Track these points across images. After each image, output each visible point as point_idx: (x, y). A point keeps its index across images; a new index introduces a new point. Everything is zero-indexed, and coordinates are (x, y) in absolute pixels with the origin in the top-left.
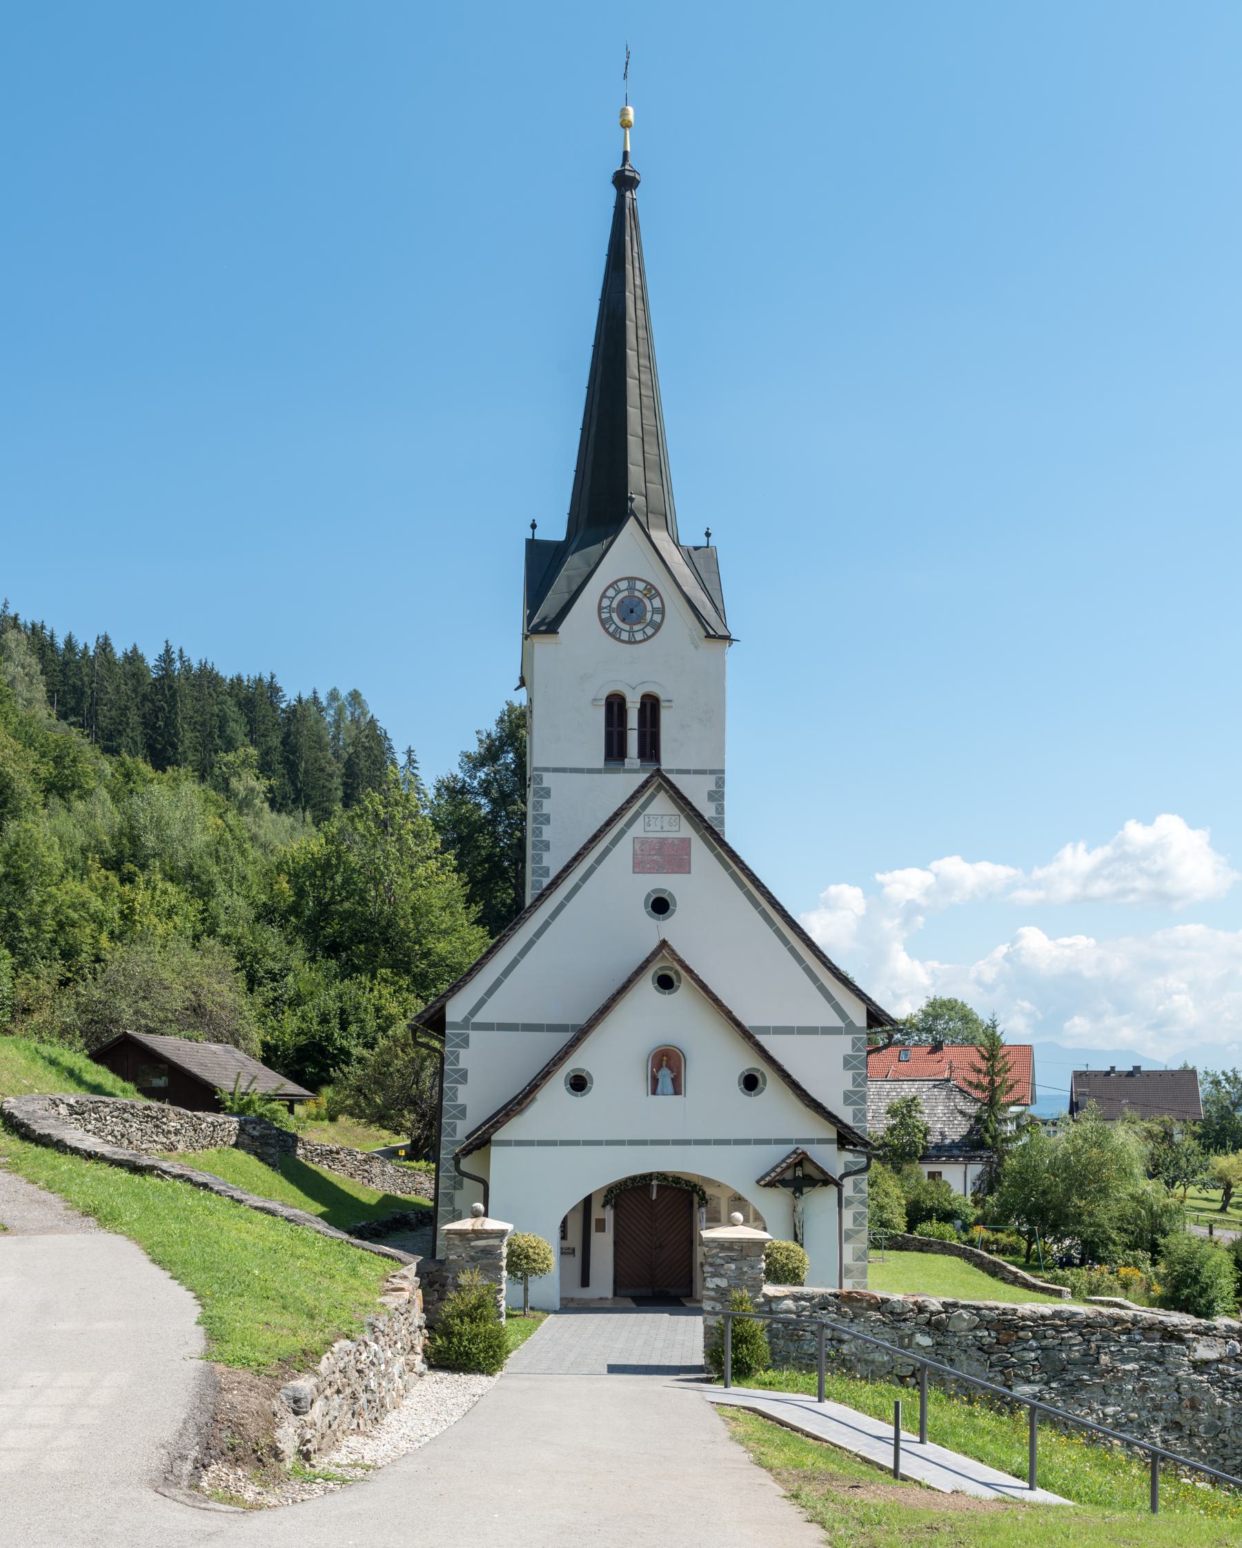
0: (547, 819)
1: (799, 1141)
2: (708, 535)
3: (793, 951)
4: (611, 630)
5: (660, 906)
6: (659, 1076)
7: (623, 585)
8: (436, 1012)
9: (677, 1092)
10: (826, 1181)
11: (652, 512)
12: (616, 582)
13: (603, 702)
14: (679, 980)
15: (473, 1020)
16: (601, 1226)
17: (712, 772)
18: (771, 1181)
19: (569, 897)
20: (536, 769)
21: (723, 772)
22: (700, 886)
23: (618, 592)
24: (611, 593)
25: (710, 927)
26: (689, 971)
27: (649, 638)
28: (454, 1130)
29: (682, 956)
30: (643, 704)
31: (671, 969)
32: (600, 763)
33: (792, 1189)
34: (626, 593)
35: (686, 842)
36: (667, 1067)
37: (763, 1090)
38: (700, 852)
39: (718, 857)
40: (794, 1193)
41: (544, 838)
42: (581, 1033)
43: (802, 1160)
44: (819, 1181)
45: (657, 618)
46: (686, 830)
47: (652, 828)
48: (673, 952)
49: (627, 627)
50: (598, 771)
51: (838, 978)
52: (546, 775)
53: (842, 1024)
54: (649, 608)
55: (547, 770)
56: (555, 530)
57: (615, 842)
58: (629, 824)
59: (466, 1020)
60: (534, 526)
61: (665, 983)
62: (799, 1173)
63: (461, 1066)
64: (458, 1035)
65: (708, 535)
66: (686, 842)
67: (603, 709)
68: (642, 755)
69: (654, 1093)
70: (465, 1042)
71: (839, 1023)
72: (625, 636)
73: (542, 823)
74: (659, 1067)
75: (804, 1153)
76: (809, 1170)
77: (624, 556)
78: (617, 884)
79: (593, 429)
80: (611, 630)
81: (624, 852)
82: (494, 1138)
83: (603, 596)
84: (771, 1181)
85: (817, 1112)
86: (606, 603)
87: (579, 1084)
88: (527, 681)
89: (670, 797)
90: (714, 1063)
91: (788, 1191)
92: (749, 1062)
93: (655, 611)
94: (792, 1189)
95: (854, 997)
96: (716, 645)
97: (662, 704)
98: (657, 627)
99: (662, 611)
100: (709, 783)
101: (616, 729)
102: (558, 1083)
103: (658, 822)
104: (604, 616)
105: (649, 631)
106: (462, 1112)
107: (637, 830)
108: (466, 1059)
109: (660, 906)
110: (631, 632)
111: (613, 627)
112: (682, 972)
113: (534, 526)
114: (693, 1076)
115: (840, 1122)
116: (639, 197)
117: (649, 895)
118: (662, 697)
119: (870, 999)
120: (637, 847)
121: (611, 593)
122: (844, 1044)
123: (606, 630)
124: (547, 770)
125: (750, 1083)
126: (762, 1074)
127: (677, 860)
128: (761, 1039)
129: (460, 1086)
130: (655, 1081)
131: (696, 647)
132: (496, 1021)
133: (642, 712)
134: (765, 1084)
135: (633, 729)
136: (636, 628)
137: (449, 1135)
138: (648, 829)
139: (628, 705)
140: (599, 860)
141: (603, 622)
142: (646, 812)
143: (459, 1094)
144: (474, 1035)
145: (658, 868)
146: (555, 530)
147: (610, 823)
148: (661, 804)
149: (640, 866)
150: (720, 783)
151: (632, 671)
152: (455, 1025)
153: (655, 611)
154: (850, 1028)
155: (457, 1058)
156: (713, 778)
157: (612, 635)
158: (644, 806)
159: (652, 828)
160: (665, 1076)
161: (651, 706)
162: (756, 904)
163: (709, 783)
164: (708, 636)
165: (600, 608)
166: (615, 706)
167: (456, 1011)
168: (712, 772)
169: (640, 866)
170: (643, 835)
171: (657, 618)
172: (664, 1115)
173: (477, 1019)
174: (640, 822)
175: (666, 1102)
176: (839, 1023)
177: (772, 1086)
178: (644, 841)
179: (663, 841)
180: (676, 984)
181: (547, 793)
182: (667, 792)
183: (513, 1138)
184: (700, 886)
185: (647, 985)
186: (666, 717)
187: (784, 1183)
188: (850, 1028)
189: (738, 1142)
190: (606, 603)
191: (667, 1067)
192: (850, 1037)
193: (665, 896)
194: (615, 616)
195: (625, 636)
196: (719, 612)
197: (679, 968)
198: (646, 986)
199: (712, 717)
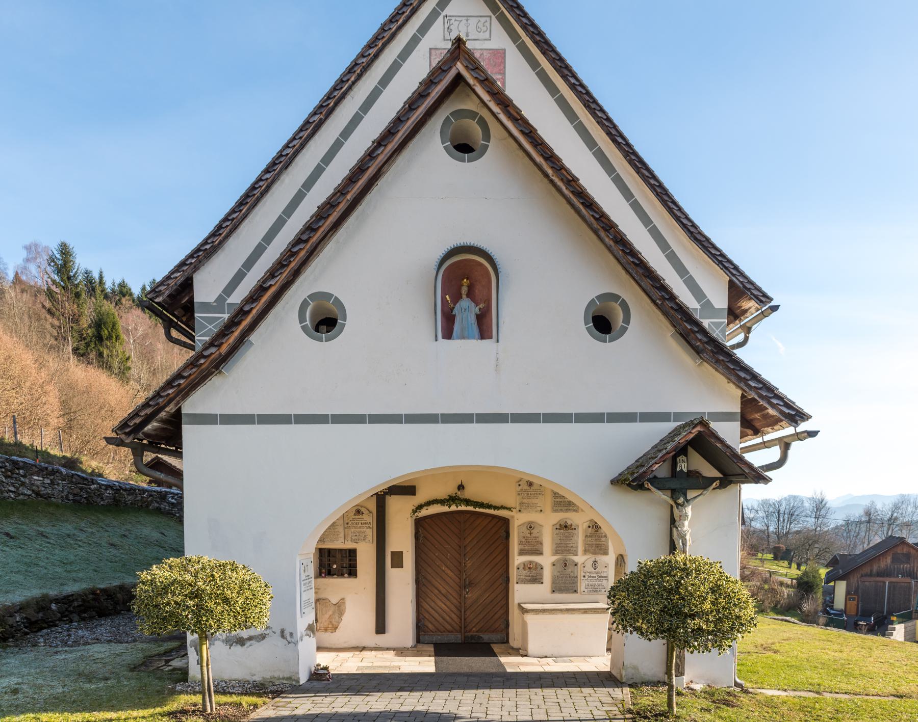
18: (634, 480)
31: (472, 115)
33: (669, 493)
36: (466, 287)
37: (624, 330)
44: (713, 480)
62: (683, 466)
69: (448, 334)
74: (457, 298)
84: (634, 480)
119: (736, 268)
160: (466, 310)
172: (465, 370)
185: (431, 147)
187: (656, 482)
189: (583, 418)
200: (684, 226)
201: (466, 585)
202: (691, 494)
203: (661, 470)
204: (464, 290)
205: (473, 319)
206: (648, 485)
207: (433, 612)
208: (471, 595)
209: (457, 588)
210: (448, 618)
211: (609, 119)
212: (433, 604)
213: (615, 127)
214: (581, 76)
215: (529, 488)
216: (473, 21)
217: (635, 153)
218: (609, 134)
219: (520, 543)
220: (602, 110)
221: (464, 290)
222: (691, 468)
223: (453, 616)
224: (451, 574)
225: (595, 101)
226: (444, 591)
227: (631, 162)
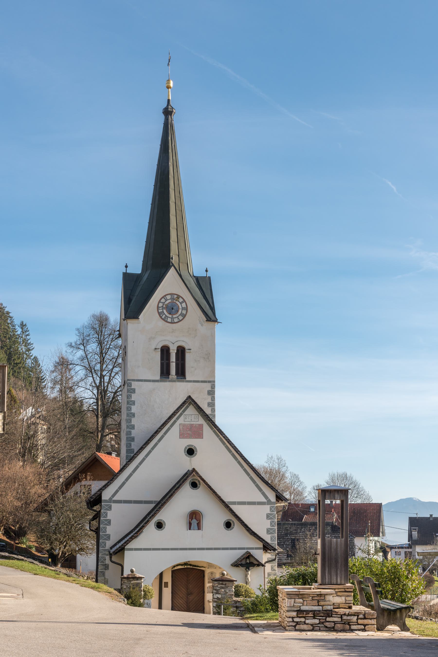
0: (134, 403)
1: (247, 548)
2: (207, 271)
3: (245, 470)
4: (163, 317)
5: (191, 452)
6: (192, 522)
7: (169, 297)
8: (98, 496)
9: (199, 528)
10: (260, 564)
11: (181, 263)
12: (165, 296)
13: (160, 350)
14: (200, 484)
15: (113, 499)
16: (166, 585)
17: (209, 382)
18: (236, 565)
19: (153, 448)
20: (128, 380)
21: (214, 382)
22: (206, 444)
23: (166, 300)
25: (211, 462)
26: (204, 481)
27: (180, 321)
28: (105, 545)
29: (201, 475)
30: (178, 350)
31: (197, 480)
32: (158, 377)
33: (245, 568)
34: (170, 301)
35: (201, 426)
36: (195, 519)
37: (233, 528)
38: (207, 430)
39: (214, 432)
40: (246, 569)
41: (132, 411)
42: (160, 505)
43: (249, 556)
44: (255, 565)
45: (184, 312)
46: (201, 421)
47: (187, 420)
48: (197, 473)
49: (170, 316)
50: (157, 381)
51: (263, 482)
52: (133, 383)
53: (266, 501)
54: (180, 307)
55: (134, 380)
56: (136, 268)
58: (178, 418)
59: (110, 499)
60: (126, 267)
61: (194, 485)
62: (248, 561)
63: (108, 518)
64: (107, 505)
65: (207, 271)
66: (201, 426)
67: (160, 352)
68: (177, 374)
69: (190, 529)
70: (110, 508)
71: (264, 500)
73: (131, 405)
75: (250, 553)
76: (252, 560)
77: (170, 284)
78: (173, 443)
79: (154, 224)
80: (163, 317)
81: (175, 430)
82: (126, 547)
84: (236, 565)
85: (255, 537)
87: (160, 525)
88: (123, 335)
89: (195, 407)
90: (214, 517)
91: (243, 569)
92: (228, 517)
93: (183, 309)
94: (245, 568)
95: (270, 489)
96: (211, 324)
97: (187, 351)
98: (184, 316)
99: (186, 309)
100: (208, 387)
101: (165, 362)
102: (152, 525)
103: (190, 418)
104: (160, 311)
105: (181, 318)
106: (108, 537)
107: (181, 421)
108: (110, 515)
109: (191, 452)
110: (172, 318)
111: (164, 316)
112: (201, 481)
113: (126, 267)
114: (205, 523)
115: (264, 540)
116: (176, 119)
117: (186, 447)
118: (187, 347)
120: (181, 428)
121: (163, 300)
122: (267, 509)
123: (161, 317)
124: (134, 380)
125: (228, 525)
126: (233, 522)
127: (197, 433)
128: (232, 506)
129: (108, 527)
130: (190, 524)
131: (202, 325)
132: (122, 499)
133: (177, 354)
134: (234, 525)
135: (173, 363)
136: (174, 316)
137: (103, 547)
138: (186, 420)
139: (171, 351)
140: (165, 433)
142: (185, 413)
143: (107, 530)
144: (113, 505)
146: (136, 268)
147: (170, 418)
149: (182, 435)
150: (213, 387)
152: (106, 501)
153: (183, 309)
154: (269, 502)
155: (107, 515)
158: (184, 411)
159: (187, 420)
162: (230, 451)
163: (208, 387)
165: (158, 307)
166: (165, 351)
167: (106, 495)
168: (209, 382)
169: (182, 435)
170: (184, 423)
171: (184, 312)
172: (194, 537)
173: (115, 498)
174: (182, 417)
175: (195, 533)
176: (264, 500)
177: (237, 526)
178: (184, 425)
179: (192, 425)
180: (198, 485)
181: (134, 391)
182: (193, 405)
183: (134, 547)
184: (206, 444)
185: (187, 487)
186: (188, 356)
187: (242, 565)
188: (269, 502)
191: (195, 519)
192: (269, 506)
193: (193, 448)
194: (165, 311)
195: (169, 320)
196: (212, 309)
197: (200, 480)
198: (187, 487)
199: (209, 357)
200: (260, 478)
201: (189, 594)
202: (250, 568)
203: (244, 562)
204: (194, 517)
205: (196, 525)
206: (239, 566)
207: (177, 604)
208: (191, 598)
209: (186, 595)
210: (183, 606)
211: (235, 447)
212: (177, 601)
213: (237, 449)
214: (226, 434)
215: (210, 565)
216: (193, 416)
217: (243, 456)
218: (235, 451)
219: (208, 579)
220: (233, 444)
221: (194, 517)
222: (251, 561)
223: (185, 605)
224: (184, 590)
225: (231, 442)
226: (181, 596)
227: (242, 459)
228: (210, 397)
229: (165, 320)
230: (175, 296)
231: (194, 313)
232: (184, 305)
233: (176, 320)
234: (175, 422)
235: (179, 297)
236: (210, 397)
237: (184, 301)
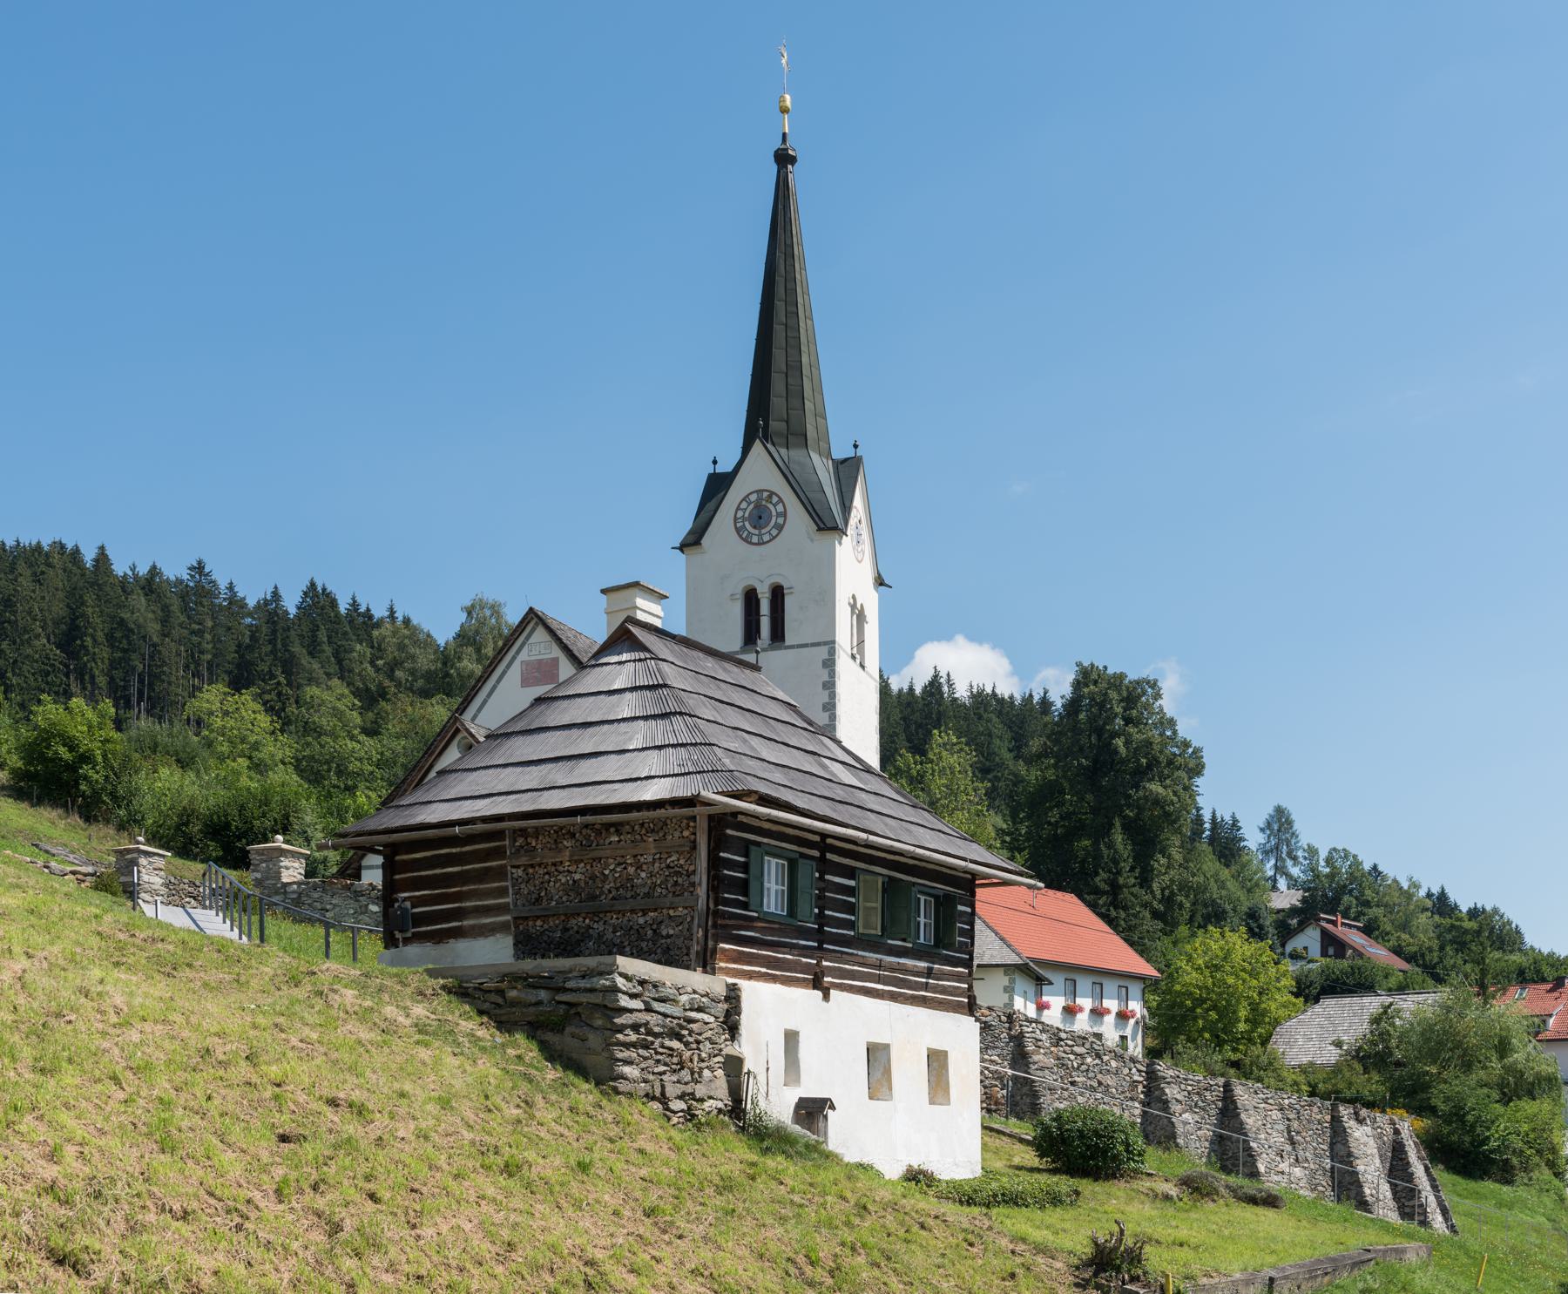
2: (856, 446)
17: (825, 643)
24: (744, 505)
35: (556, 660)
45: (781, 520)
46: (556, 652)
57: (508, 666)
58: (518, 652)
60: (715, 462)
65: (856, 446)
66: (556, 660)
72: (755, 539)
81: (515, 673)
83: (738, 508)
86: (740, 514)
93: (778, 515)
98: (780, 528)
99: (784, 514)
100: (823, 652)
105: (774, 532)
107: (523, 656)
110: (760, 535)
113: (715, 462)
140: (499, 681)
141: (738, 530)
142: (531, 640)
145: (537, 682)
148: (540, 635)
149: (526, 682)
151: (760, 567)
153: (778, 515)
156: (825, 649)
157: (745, 540)
158: (528, 638)
161: (778, 594)
163: (823, 652)
164: (820, 529)
165: (736, 519)
166: (751, 598)
169: (526, 682)
186: (790, 603)
190: (740, 514)
195: (755, 539)
228: (826, 672)
229: (747, 541)
230: (765, 494)
231: (798, 518)
232: (780, 508)
233: (766, 538)
234: (514, 658)
235: (772, 493)
236: (826, 672)
237: (781, 500)
